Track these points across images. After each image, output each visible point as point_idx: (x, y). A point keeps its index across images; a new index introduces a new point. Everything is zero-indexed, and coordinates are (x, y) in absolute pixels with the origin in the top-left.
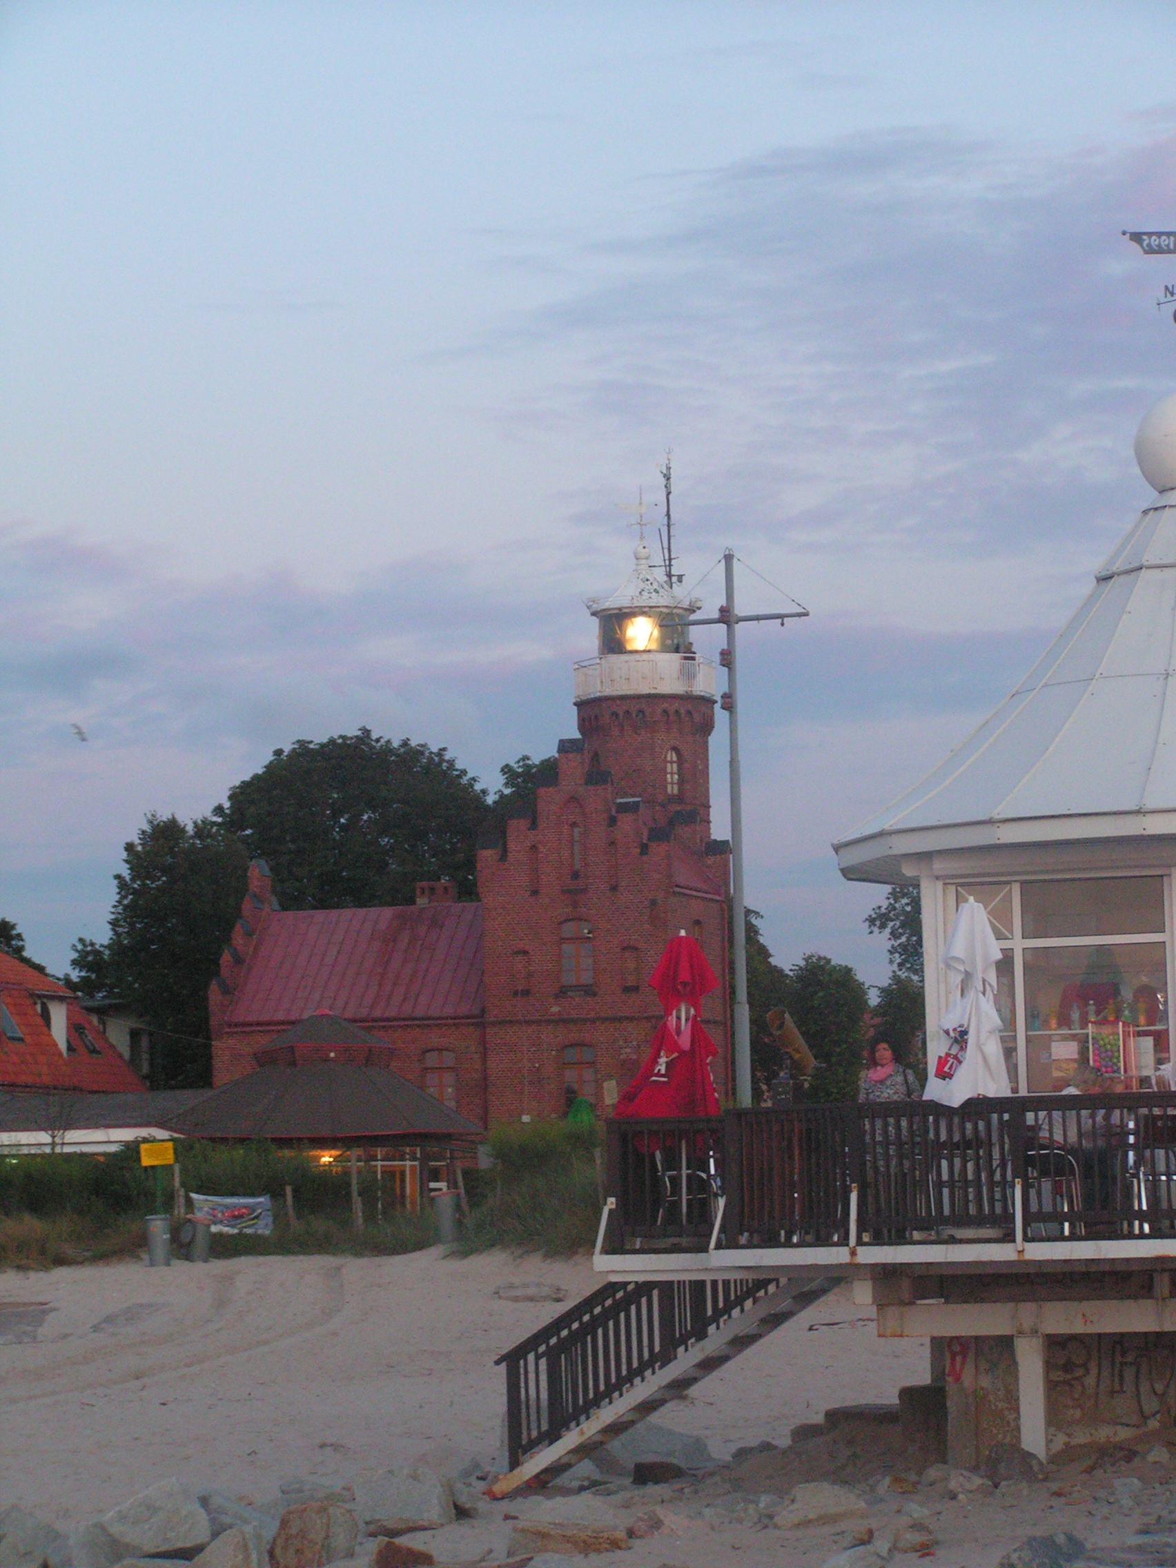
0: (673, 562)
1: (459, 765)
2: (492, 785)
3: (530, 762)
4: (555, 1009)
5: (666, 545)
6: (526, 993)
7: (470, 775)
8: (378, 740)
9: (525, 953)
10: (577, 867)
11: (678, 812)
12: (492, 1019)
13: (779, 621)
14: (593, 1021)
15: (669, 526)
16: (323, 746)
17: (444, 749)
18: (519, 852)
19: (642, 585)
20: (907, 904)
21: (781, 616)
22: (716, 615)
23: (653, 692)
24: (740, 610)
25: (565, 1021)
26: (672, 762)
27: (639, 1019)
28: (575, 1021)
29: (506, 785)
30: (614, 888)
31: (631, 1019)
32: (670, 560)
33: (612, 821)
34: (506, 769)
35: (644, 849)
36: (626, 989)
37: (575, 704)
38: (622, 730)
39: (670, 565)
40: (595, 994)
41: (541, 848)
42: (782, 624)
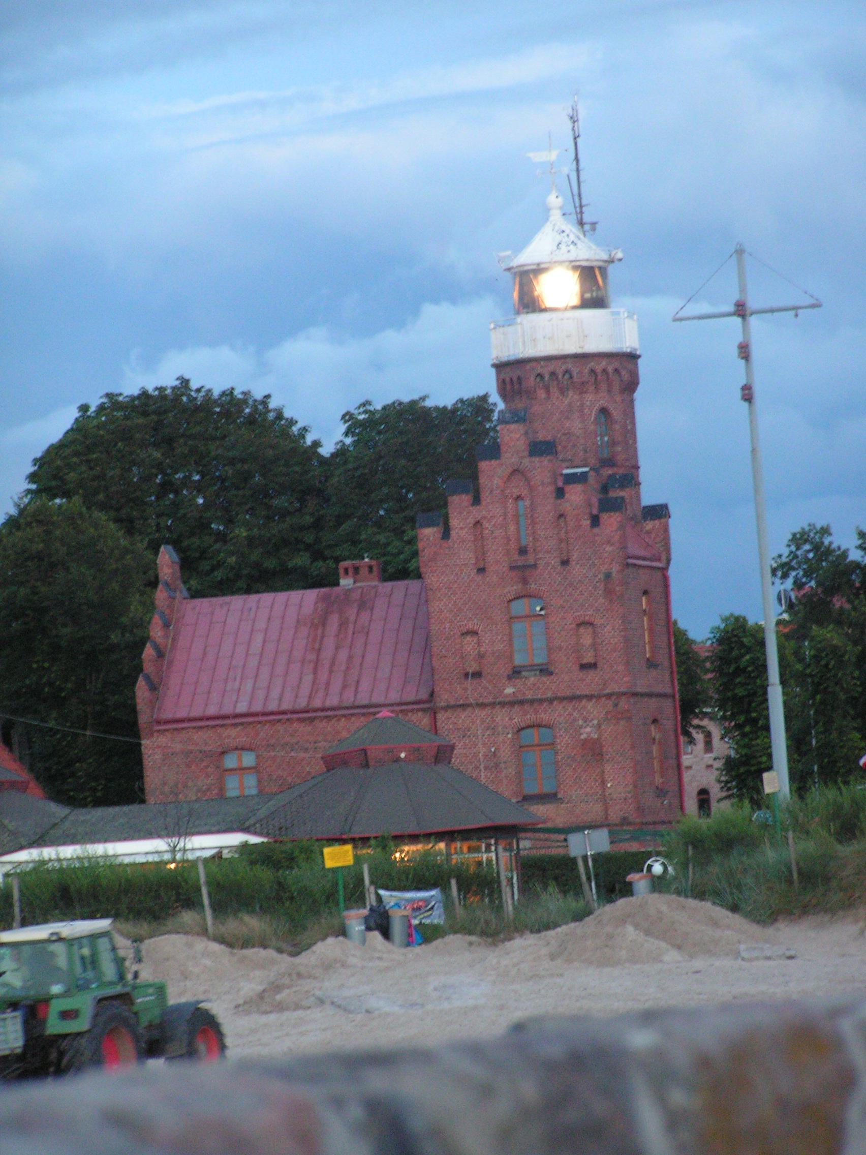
0: (584, 209)
1: (287, 414)
2: (330, 437)
3: (371, 408)
4: (509, 690)
6: (477, 675)
7: (300, 425)
8: (198, 390)
9: (475, 633)
10: (524, 542)
11: (610, 476)
12: (443, 704)
13: (793, 313)
14: (551, 701)
15: (578, 170)
16: (133, 398)
17: (268, 397)
18: (462, 528)
19: (558, 238)
20: (809, 551)
21: (796, 308)
22: (731, 308)
23: (580, 351)
24: (753, 303)
25: (521, 702)
27: (599, 697)
28: (532, 702)
29: (346, 434)
30: (565, 563)
31: (590, 697)
32: (581, 206)
33: (560, 493)
34: (347, 417)
35: (595, 521)
36: (584, 667)
37: (495, 366)
38: (548, 392)
39: (581, 213)
40: (551, 674)
41: (485, 524)
42: (797, 315)
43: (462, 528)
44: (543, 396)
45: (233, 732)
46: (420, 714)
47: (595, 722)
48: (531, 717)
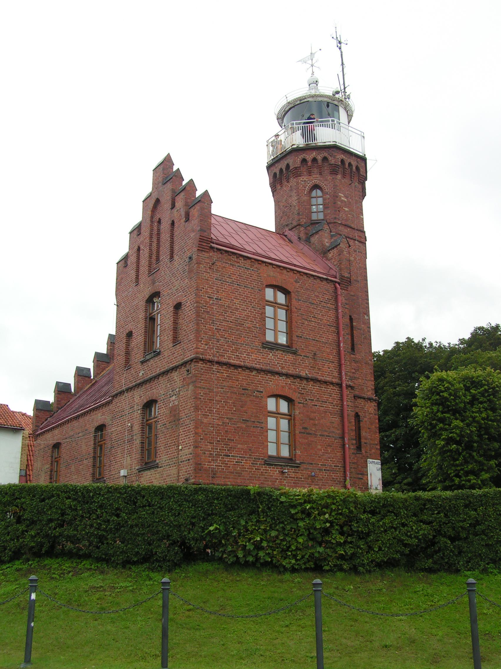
0: (347, 90)
5: (342, 83)
14: (157, 377)
26: (317, 197)
30: (172, 257)
38: (281, 184)
41: (142, 247)
44: (279, 187)
45: (56, 432)
47: (177, 390)
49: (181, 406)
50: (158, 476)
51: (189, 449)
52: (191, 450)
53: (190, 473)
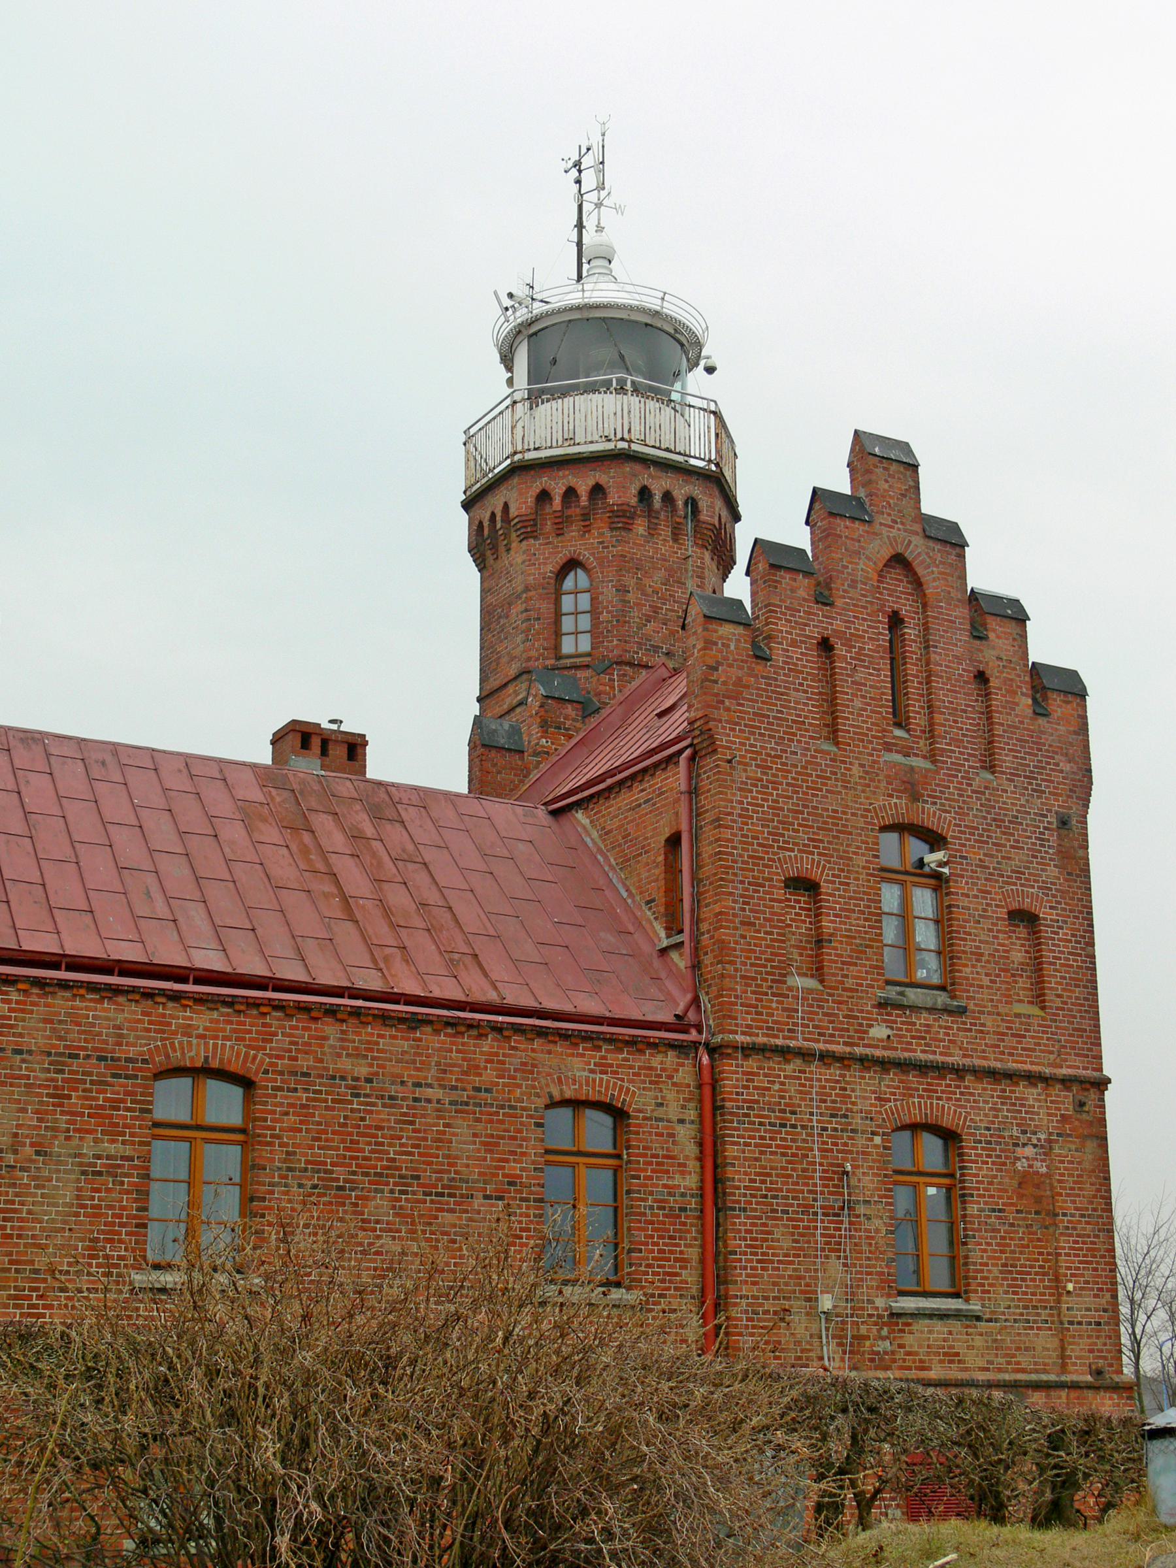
4: (879, 1032)
14: (959, 1072)
18: (794, 643)
25: (904, 1066)
28: (923, 1068)
31: (1032, 1078)
43: (794, 643)
45: (202, 1019)
46: (671, 1057)
47: (1043, 1137)
48: (917, 1108)
49: (1060, 1181)
50: (979, 1341)
51: (1096, 1296)
52: (1104, 1301)
53: (1105, 1358)
